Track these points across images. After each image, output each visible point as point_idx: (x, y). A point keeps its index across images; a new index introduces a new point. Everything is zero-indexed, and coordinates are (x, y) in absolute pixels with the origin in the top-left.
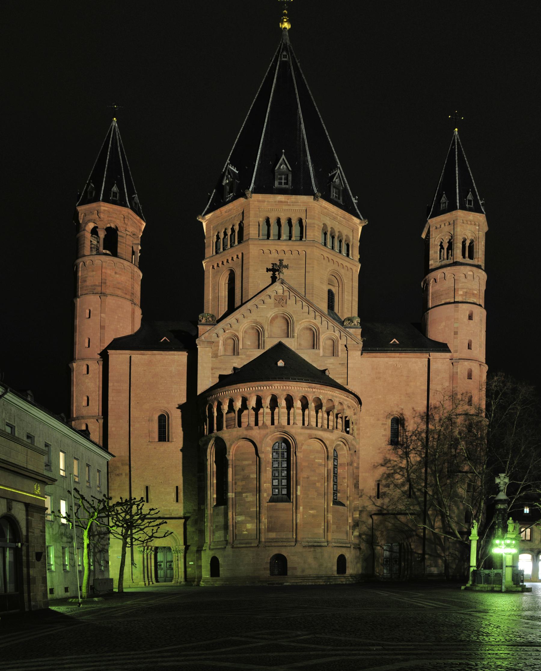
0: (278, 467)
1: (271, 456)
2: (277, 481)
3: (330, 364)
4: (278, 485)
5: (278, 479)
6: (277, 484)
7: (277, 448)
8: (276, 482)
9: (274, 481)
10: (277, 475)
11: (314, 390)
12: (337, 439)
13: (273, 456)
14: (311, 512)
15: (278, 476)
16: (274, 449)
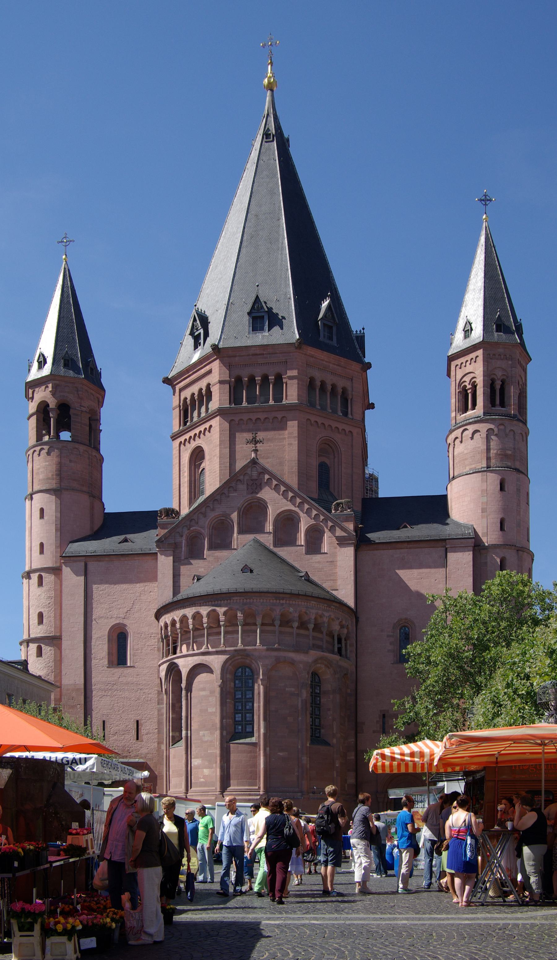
0: (242, 698)
1: (232, 684)
2: (240, 715)
3: (316, 562)
4: (242, 721)
5: (242, 714)
6: (240, 719)
7: (240, 674)
8: (239, 717)
9: (237, 716)
10: (240, 708)
11: (281, 602)
12: (315, 661)
13: (235, 685)
14: (281, 754)
15: (242, 710)
16: (237, 676)
